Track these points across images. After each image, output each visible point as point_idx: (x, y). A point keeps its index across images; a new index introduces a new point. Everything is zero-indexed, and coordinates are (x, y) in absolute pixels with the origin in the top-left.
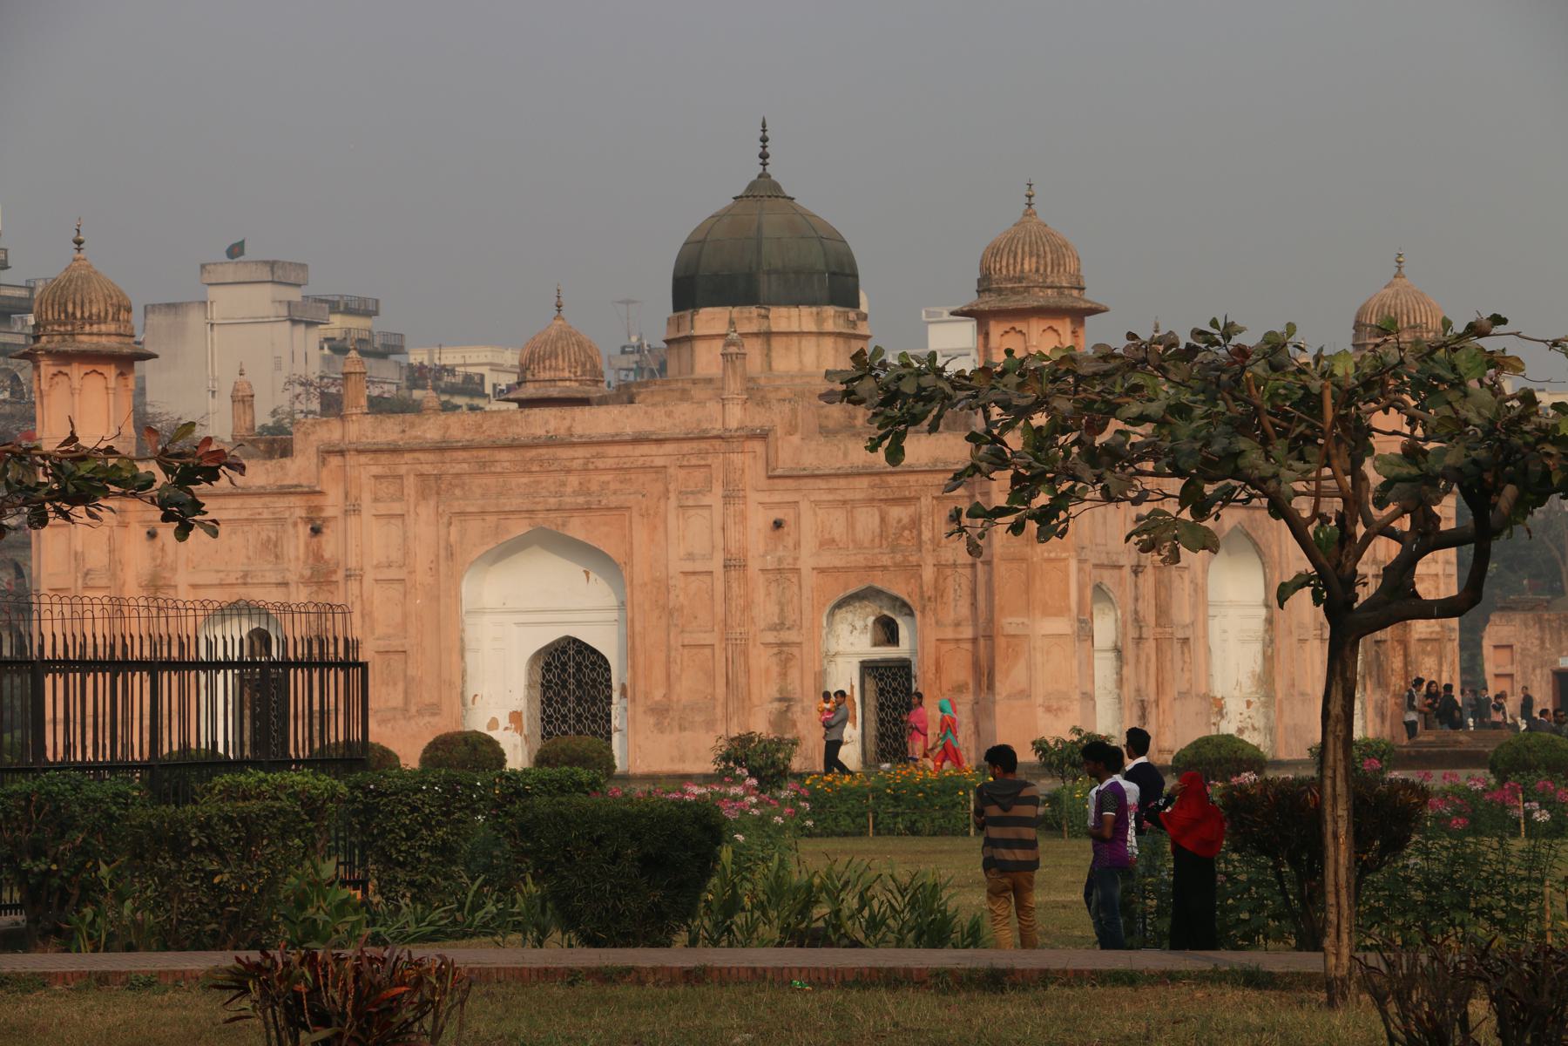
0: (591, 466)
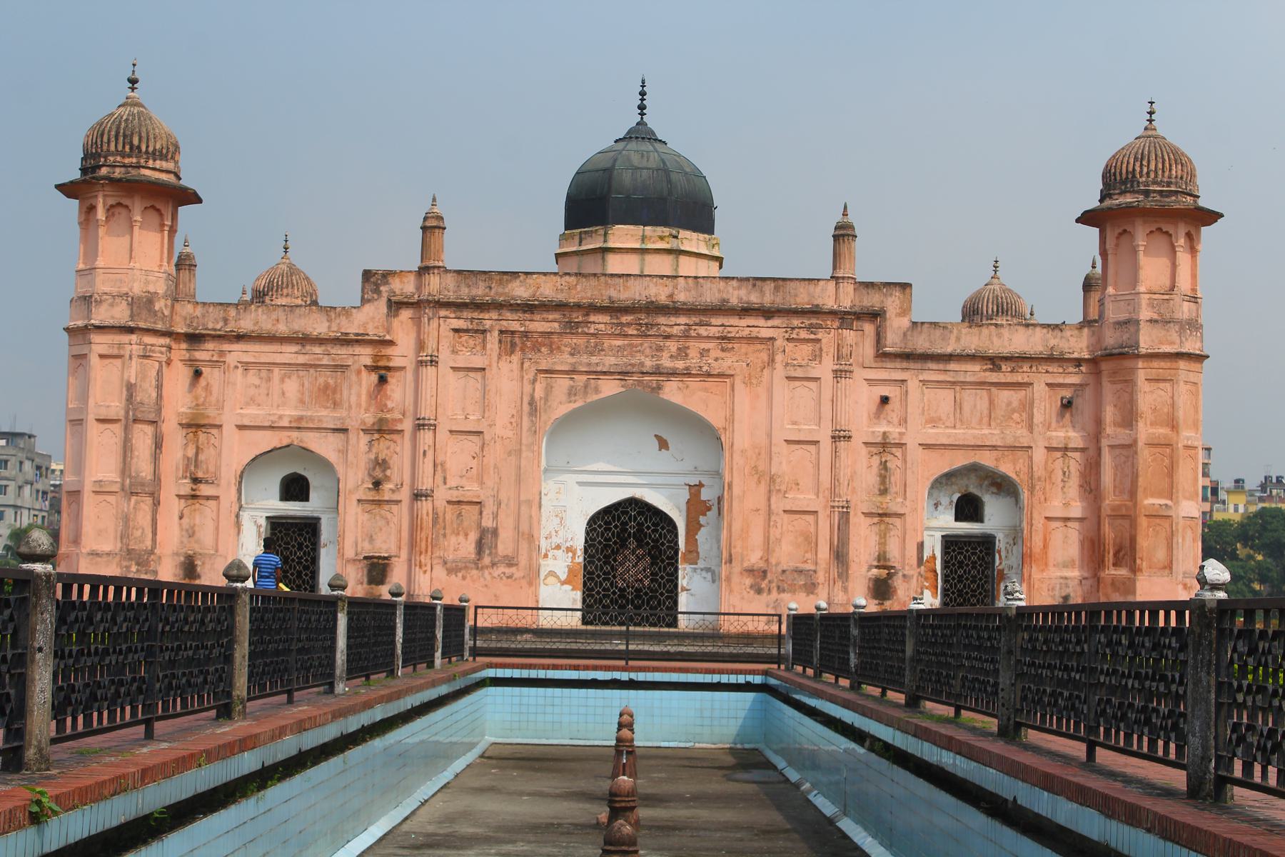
0: (693, 333)
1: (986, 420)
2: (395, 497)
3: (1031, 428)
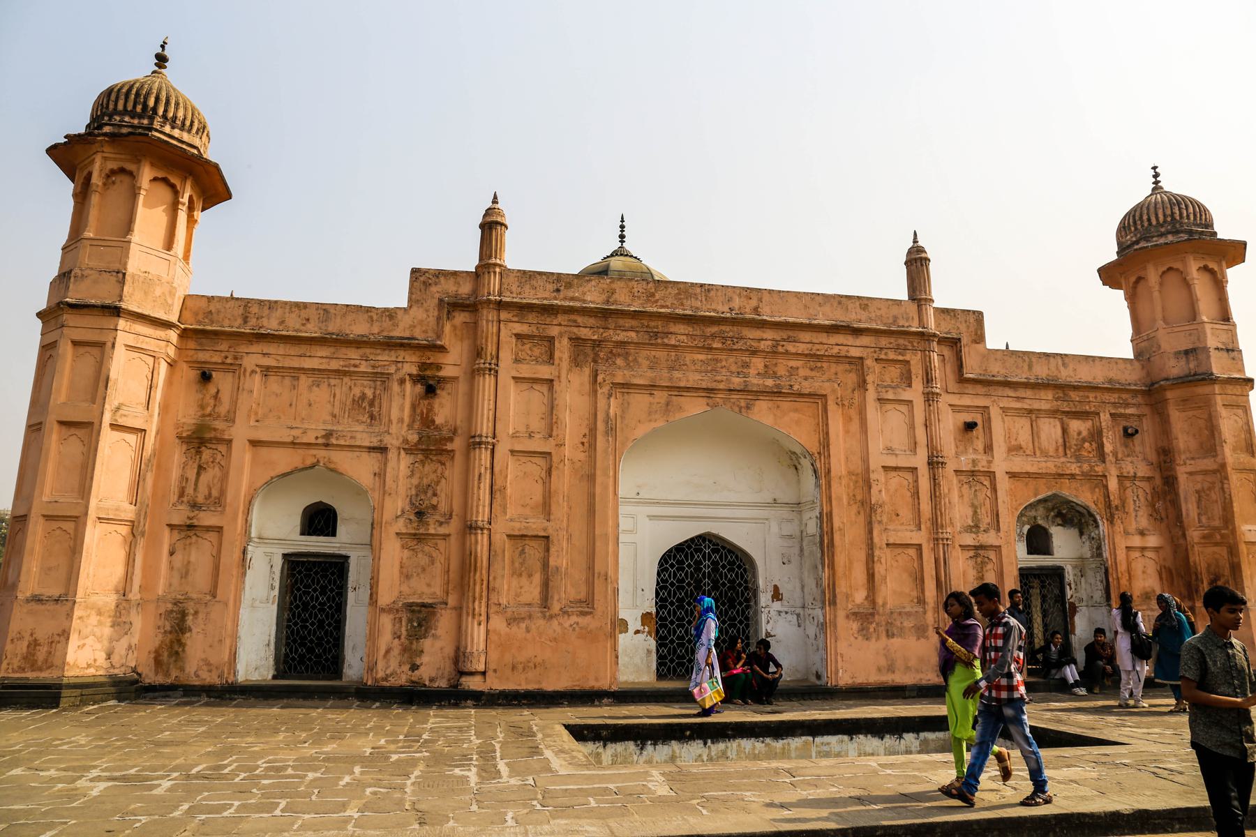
0: (780, 349)
1: (1061, 449)
2: (442, 530)
3: (1102, 457)
